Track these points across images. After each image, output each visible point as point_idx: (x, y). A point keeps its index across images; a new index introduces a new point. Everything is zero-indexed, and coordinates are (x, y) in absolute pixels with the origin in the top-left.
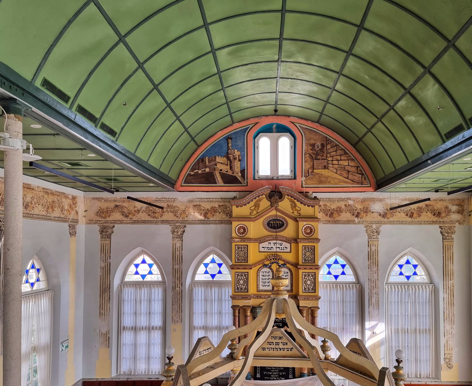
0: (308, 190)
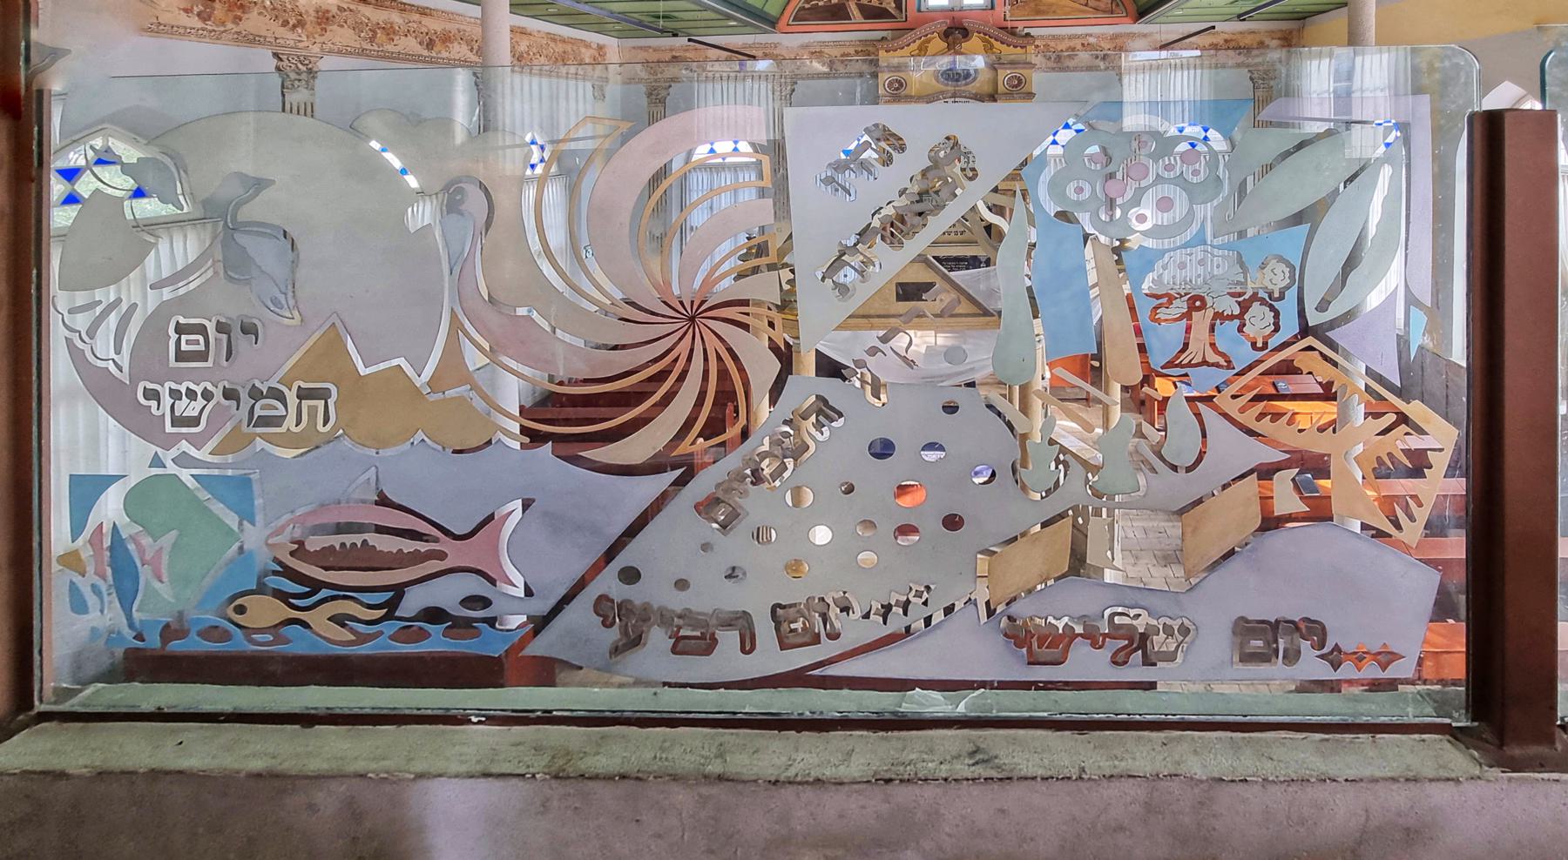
0: (1015, 24)
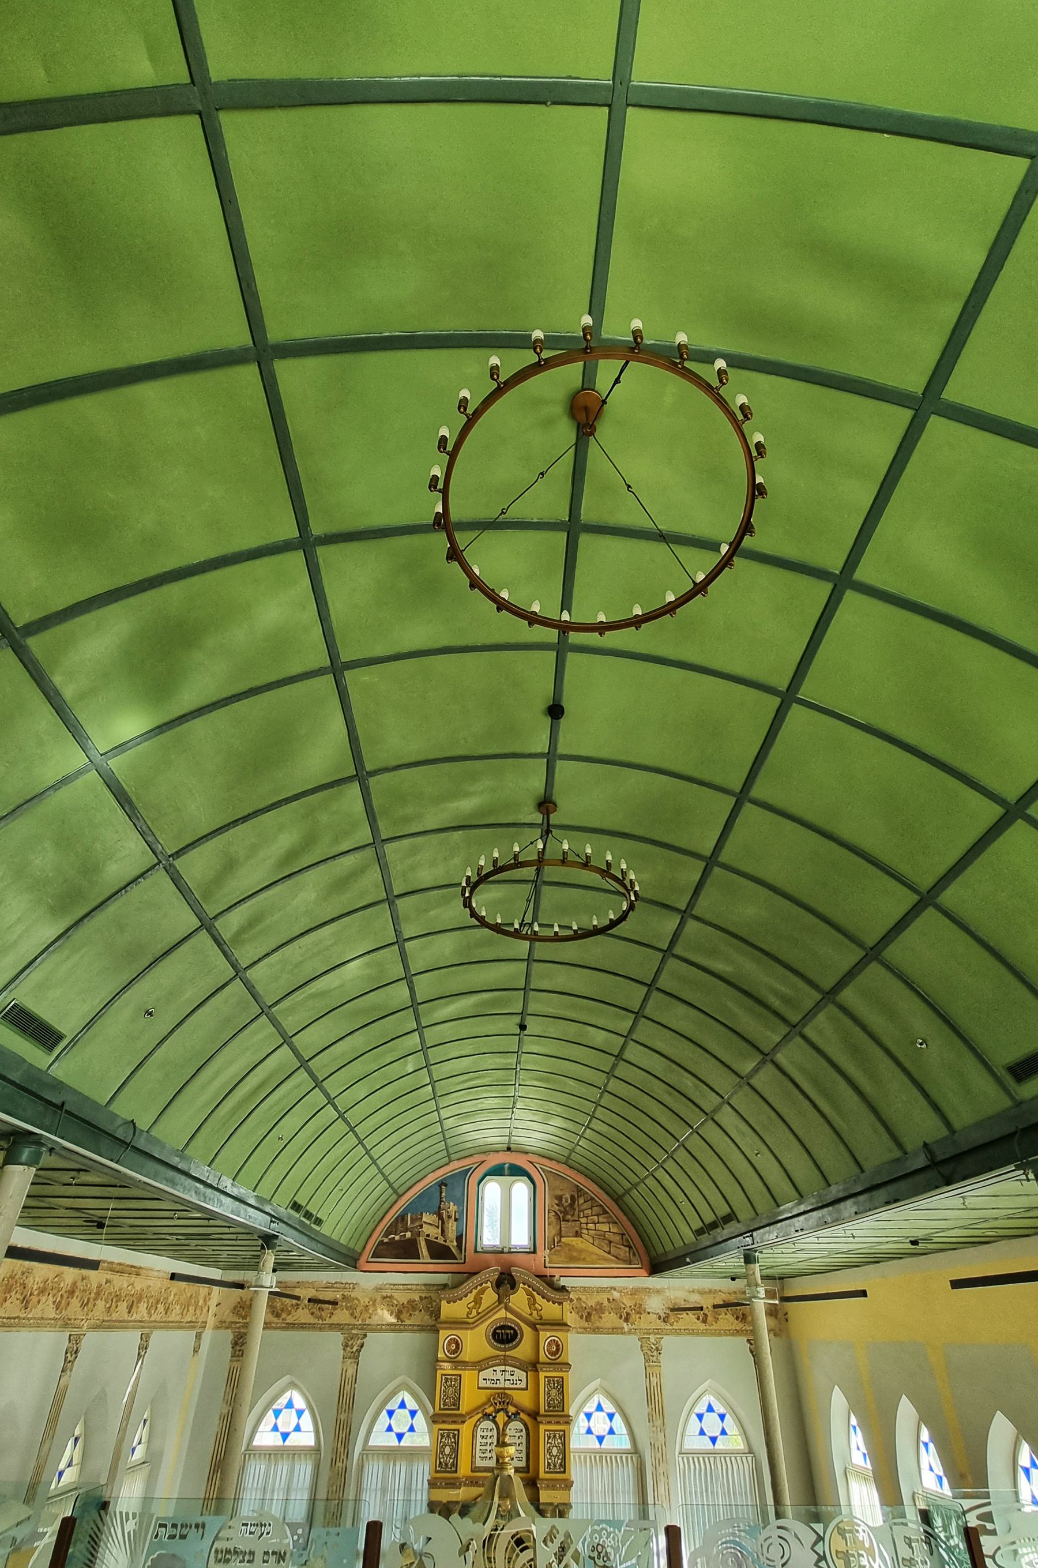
0: (553, 1272)
